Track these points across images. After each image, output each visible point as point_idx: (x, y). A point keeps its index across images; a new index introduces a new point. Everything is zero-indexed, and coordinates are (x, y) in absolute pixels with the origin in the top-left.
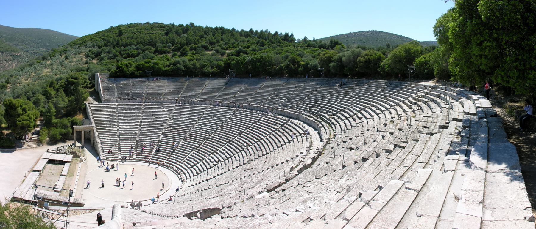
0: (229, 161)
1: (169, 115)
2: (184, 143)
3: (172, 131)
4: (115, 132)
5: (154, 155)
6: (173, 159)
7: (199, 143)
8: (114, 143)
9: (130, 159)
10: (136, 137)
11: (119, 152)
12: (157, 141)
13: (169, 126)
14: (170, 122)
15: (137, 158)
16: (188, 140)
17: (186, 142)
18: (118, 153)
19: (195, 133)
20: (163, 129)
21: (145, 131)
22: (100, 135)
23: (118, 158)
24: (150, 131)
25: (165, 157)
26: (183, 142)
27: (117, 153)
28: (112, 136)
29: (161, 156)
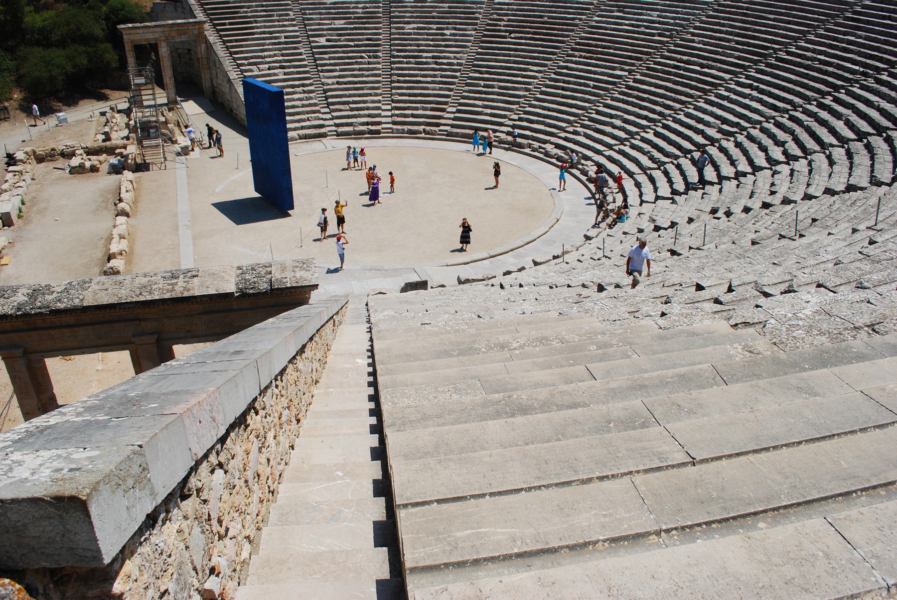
3: (511, 32)
4: (292, 42)
5: (459, 111)
6: (537, 122)
7: (627, 68)
8: (299, 79)
9: (371, 132)
10: (380, 54)
11: (323, 110)
13: (495, 16)
15: (399, 127)
16: (580, 57)
18: (319, 112)
19: (603, 34)
20: (476, 24)
21: (409, 34)
23: (323, 130)
24: (428, 34)
25: (504, 117)
27: (314, 112)
28: (283, 55)
29: (486, 114)
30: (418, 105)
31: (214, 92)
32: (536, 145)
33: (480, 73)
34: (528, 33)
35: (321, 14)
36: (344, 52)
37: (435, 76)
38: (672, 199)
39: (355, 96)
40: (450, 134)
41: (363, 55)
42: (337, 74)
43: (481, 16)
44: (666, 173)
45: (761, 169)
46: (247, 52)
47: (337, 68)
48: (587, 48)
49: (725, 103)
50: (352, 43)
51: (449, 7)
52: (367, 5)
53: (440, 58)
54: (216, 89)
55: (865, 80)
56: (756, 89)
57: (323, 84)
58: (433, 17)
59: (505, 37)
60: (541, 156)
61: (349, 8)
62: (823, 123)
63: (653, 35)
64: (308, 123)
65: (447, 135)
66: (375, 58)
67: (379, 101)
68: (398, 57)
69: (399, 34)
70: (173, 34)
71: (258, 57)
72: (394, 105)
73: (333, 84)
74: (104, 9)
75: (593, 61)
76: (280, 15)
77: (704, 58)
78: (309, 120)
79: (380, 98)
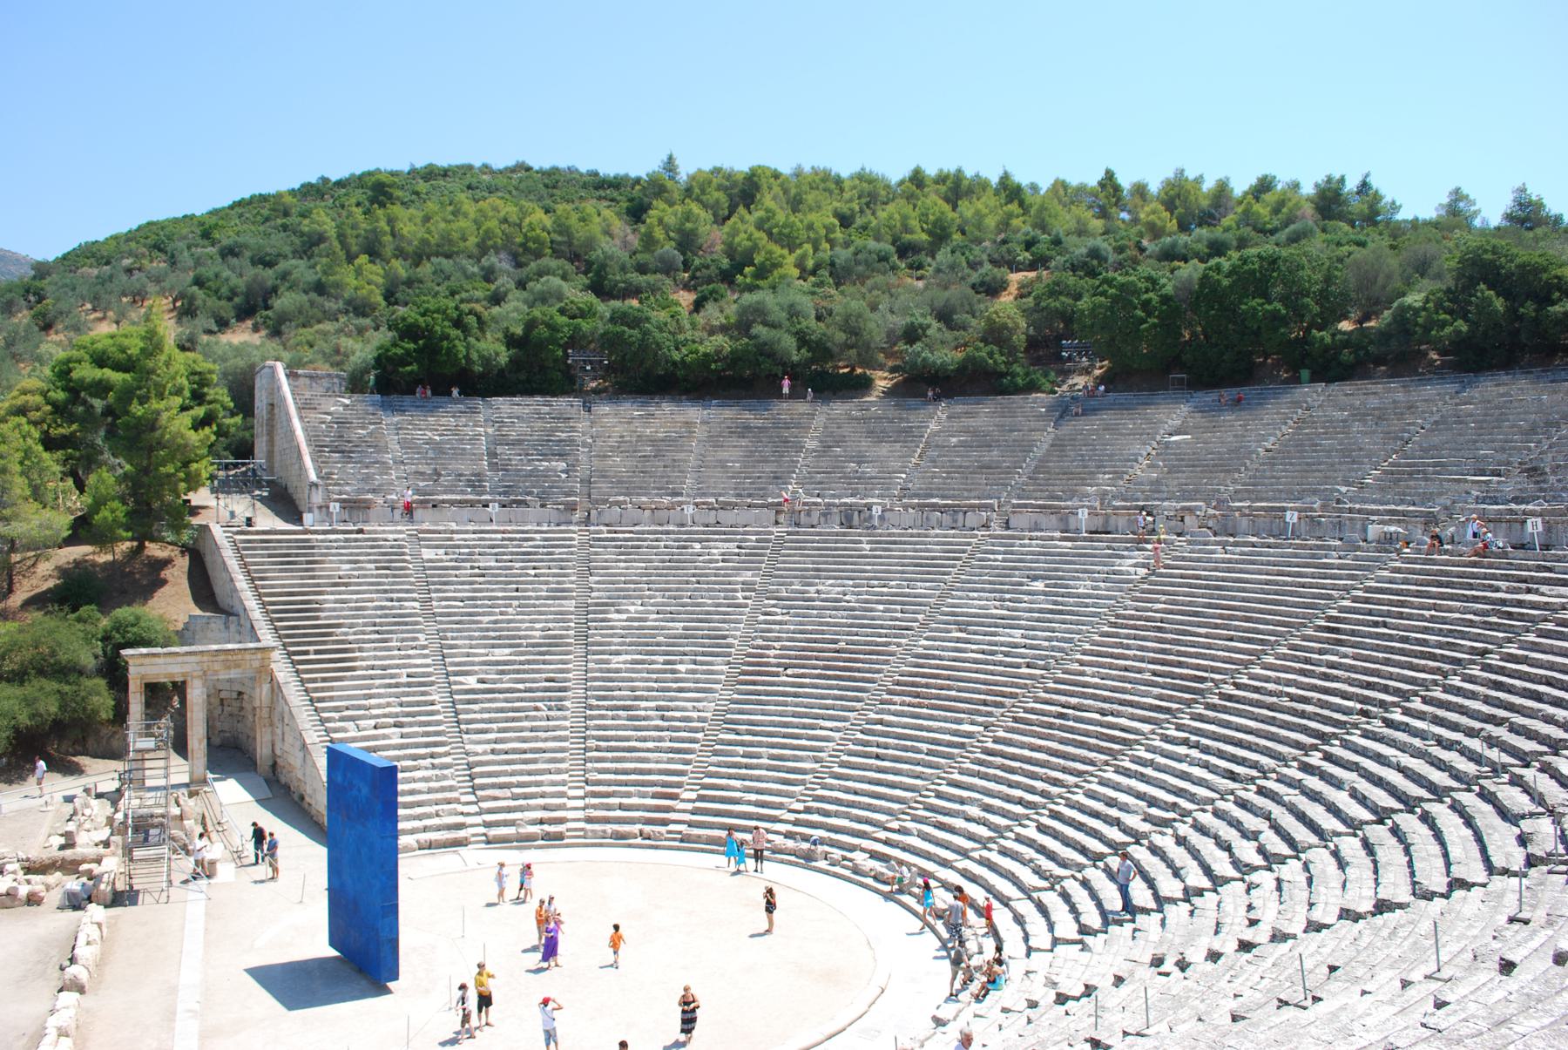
1: (748, 587)
4: (420, 683)
5: (702, 798)
6: (837, 815)
7: (981, 719)
8: (427, 745)
9: (547, 836)
10: (567, 703)
11: (464, 798)
12: (700, 720)
13: (760, 642)
14: (762, 618)
16: (903, 704)
18: (457, 801)
19: (938, 667)
20: (729, 655)
21: (618, 671)
23: (462, 834)
25: (780, 806)
29: (749, 803)
30: (632, 789)
31: (274, 766)
32: (837, 853)
33: (737, 734)
34: (815, 668)
35: (471, 638)
36: (506, 701)
37: (661, 739)
38: (1081, 942)
39: (521, 773)
40: (685, 839)
41: (540, 704)
43: (736, 642)
44: (1066, 896)
45: (1227, 880)
46: (341, 698)
47: (494, 726)
48: (910, 688)
49: (1149, 771)
50: (521, 686)
51: (685, 628)
52: (550, 625)
53: (669, 709)
54: (278, 760)
55: (1368, 723)
56: (1196, 746)
57: (467, 754)
58: (658, 644)
59: (777, 674)
60: (847, 873)
61: (519, 629)
62: (1315, 797)
63: (1018, 666)
64: (436, 821)
65: (682, 841)
66: (559, 710)
67: (564, 783)
68: (599, 708)
69: (601, 671)
70: (217, 666)
71: (359, 708)
72: (589, 788)
73: (485, 753)
74: (105, 622)
75: (925, 711)
76: (403, 640)
77: (1105, 699)
78: (438, 815)
79: (565, 777)
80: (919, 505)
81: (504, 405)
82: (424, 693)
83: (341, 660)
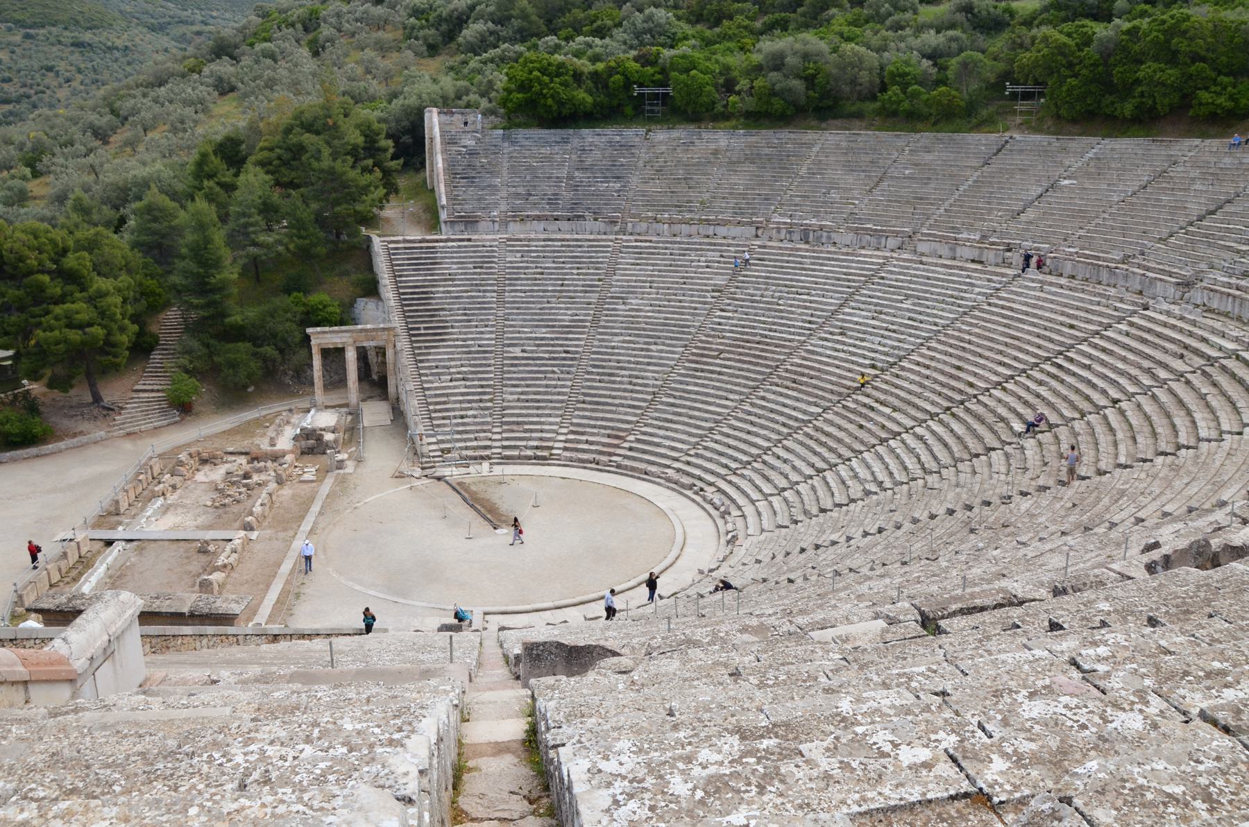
0: (929, 485)
2: (763, 398)
3: (722, 352)
5: (638, 441)
14: (719, 313)
17: (772, 397)
22: (421, 361)
23: (487, 452)
26: (762, 394)
31: (398, 399)
35: (525, 320)
42: (519, 390)
50: (546, 356)
64: (475, 443)
72: (572, 428)
80: (857, 229)
81: (589, 136)
82: (485, 358)
83: (438, 334)
